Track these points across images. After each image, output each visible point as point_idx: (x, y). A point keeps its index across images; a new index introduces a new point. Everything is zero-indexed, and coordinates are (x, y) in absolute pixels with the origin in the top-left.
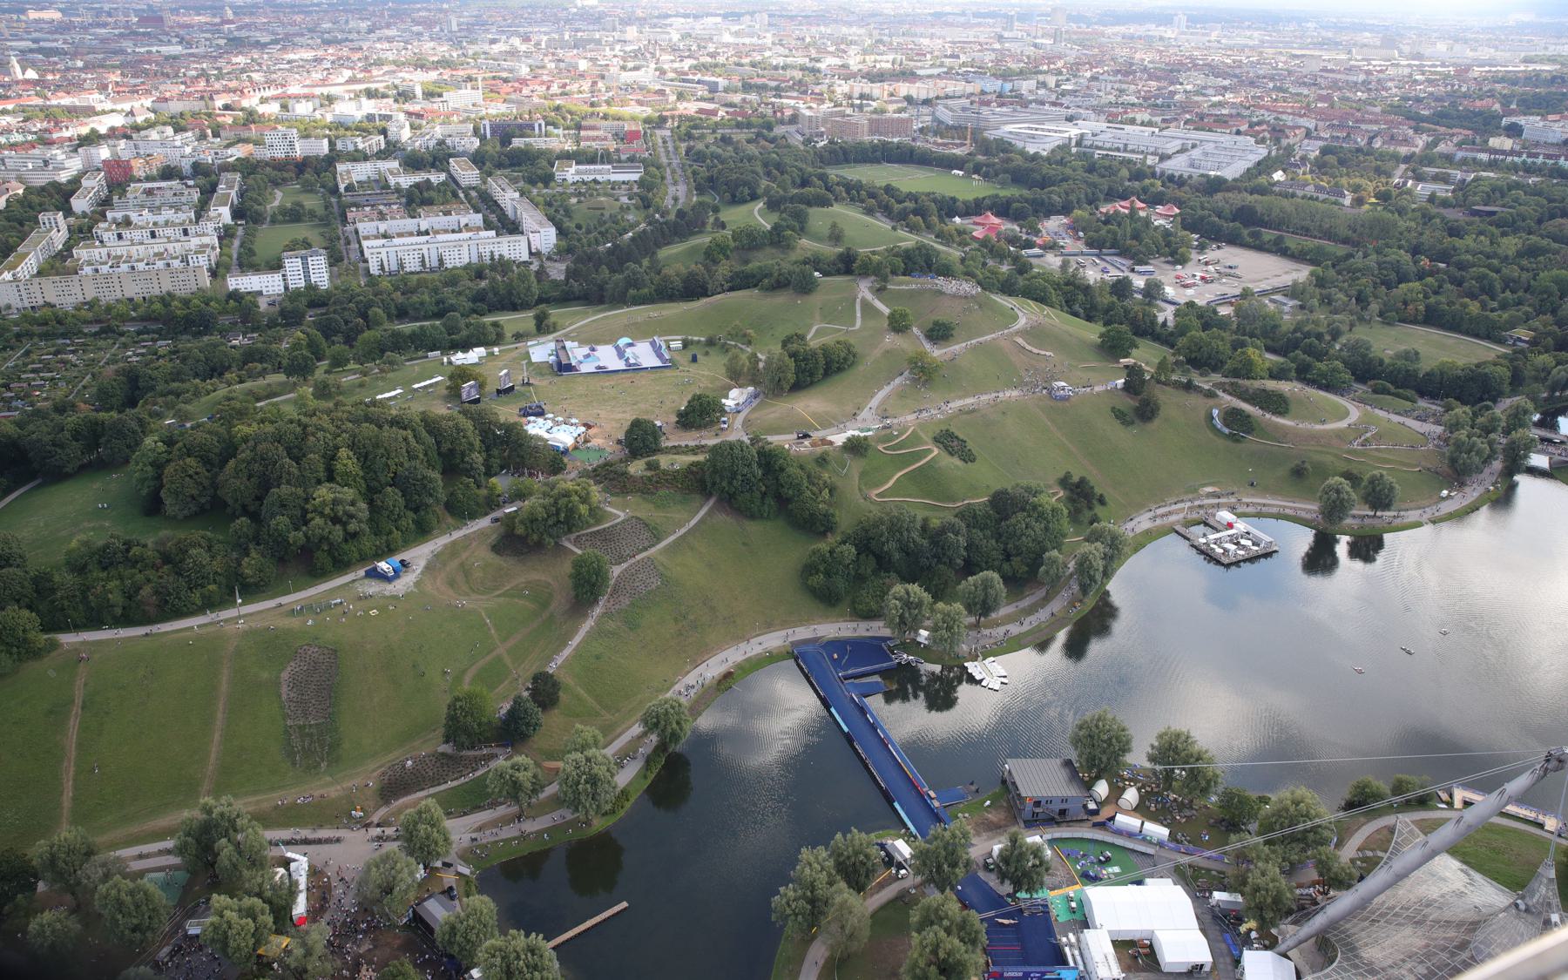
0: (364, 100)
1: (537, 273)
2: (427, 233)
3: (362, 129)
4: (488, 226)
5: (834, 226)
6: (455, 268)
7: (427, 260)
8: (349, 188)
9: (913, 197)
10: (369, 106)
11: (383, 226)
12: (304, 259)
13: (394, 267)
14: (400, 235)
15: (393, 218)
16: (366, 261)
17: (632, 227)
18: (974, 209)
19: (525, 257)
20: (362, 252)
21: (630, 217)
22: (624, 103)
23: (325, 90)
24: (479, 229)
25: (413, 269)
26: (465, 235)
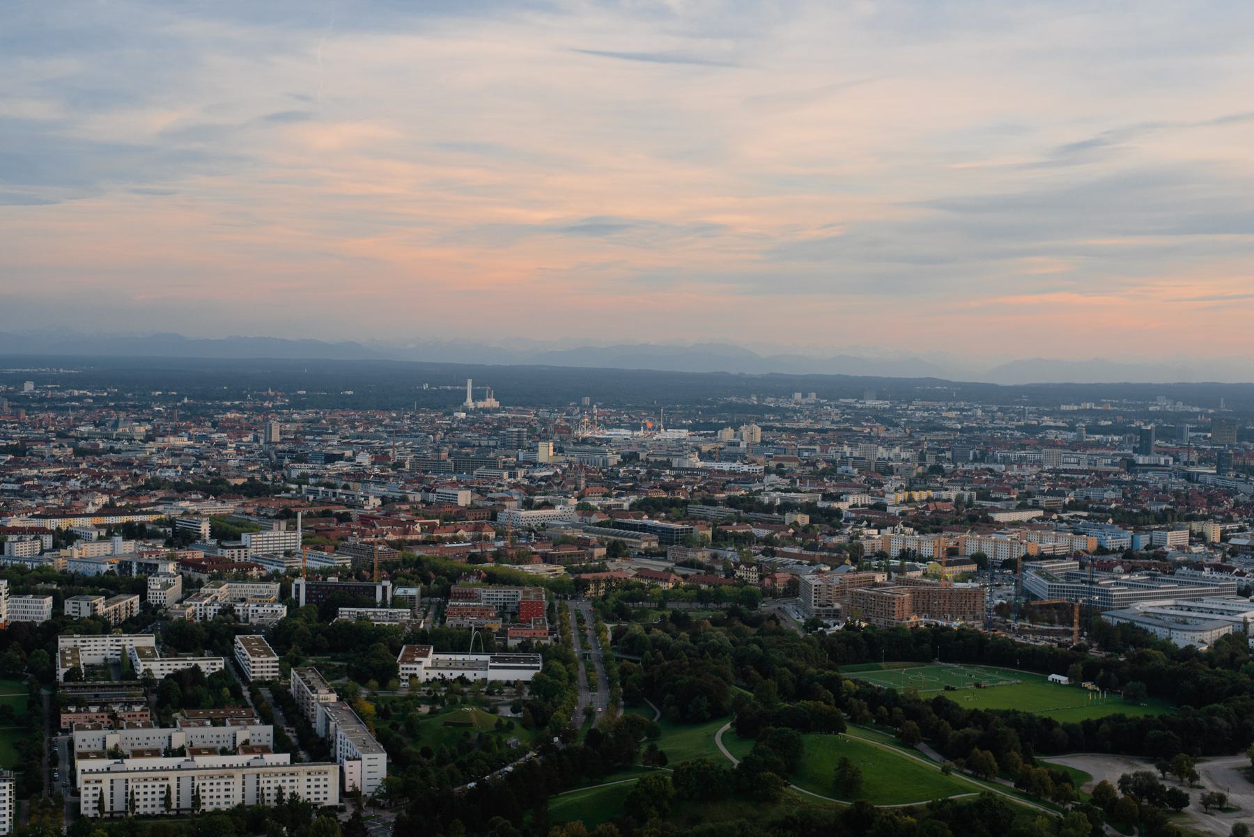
0: (118, 539)
1: (347, 825)
2: (180, 752)
3: (109, 585)
4: (280, 745)
5: (844, 764)
6: (217, 812)
7: (174, 796)
8: (72, 675)
9: (977, 717)
10: (125, 547)
11: (113, 739)
13: (120, 805)
14: (138, 754)
15: (131, 726)
16: (77, 793)
17: (514, 756)
19: (333, 798)
20: (73, 778)
21: (512, 740)
22: (523, 558)
23: (63, 524)
24: (265, 750)
25: (149, 810)
26: (241, 759)
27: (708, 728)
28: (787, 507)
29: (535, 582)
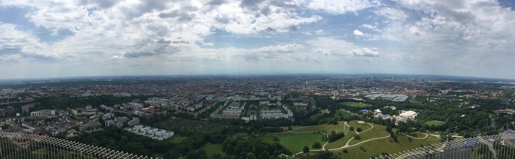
0: (265, 92)
2: (272, 113)
3: (264, 96)
4: (282, 112)
8: (261, 105)
9: (353, 107)
10: (266, 93)
11: (265, 112)
12: (253, 115)
14: (268, 113)
16: (262, 117)
18: (364, 108)
19: (288, 118)
20: (262, 115)
22: (306, 93)
24: (280, 113)
26: (278, 114)
27: (325, 110)
28: (332, 87)
29: (307, 95)
